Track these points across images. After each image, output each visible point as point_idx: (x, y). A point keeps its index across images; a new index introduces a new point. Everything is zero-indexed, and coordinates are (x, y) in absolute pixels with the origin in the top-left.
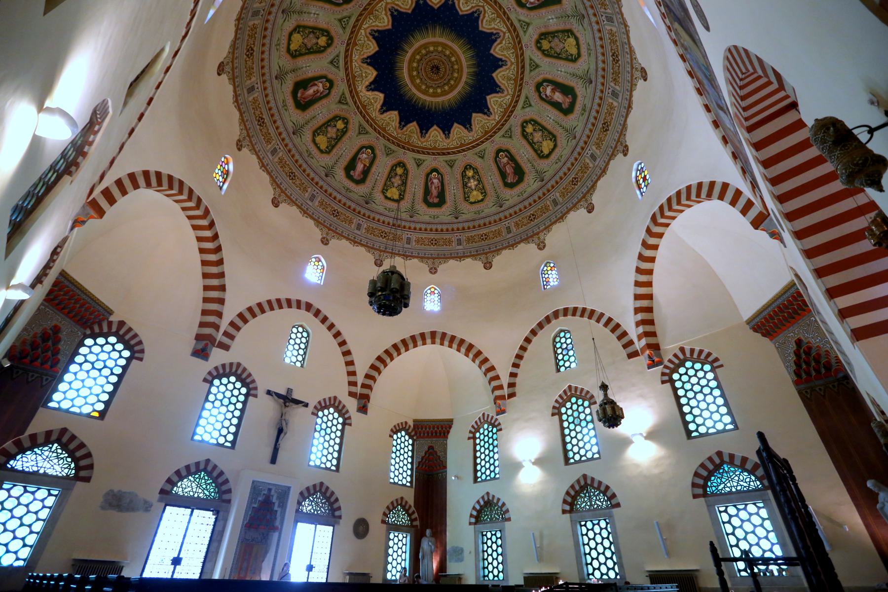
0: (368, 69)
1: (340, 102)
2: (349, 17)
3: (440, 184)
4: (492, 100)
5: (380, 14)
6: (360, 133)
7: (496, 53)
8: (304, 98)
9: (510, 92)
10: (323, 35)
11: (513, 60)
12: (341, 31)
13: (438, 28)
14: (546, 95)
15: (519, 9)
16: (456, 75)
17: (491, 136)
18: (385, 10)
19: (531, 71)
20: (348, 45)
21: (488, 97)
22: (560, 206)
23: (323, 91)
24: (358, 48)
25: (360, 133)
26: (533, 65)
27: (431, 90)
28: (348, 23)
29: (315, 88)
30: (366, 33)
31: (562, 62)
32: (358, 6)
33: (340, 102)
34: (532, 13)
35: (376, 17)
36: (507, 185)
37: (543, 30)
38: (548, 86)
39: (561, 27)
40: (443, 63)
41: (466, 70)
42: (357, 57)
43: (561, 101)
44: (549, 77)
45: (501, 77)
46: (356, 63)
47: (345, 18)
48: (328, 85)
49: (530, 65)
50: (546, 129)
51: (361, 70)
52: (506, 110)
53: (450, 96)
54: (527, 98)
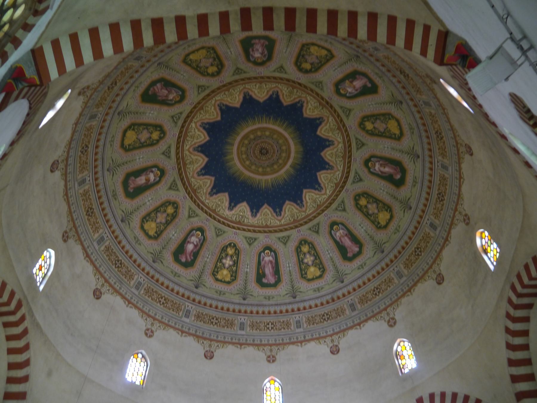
0: (329, 160)
1: (363, 144)
2: (337, 209)
3: (251, 53)
4: (203, 137)
6: (350, 110)
7: (208, 179)
8: (395, 170)
9: (187, 153)
10: (361, 206)
11: (193, 180)
12: (346, 201)
14: (152, 172)
15: (200, 224)
16: (243, 149)
17: (195, 107)
18: (307, 206)
19: (174, 181)
20: (343, 187)
21: (208, 138)
22: (86, 122)
23: (377, 162)
25: (350, 110)
27: (267, 133)
29: (382, 169)
30: (326, 190)
31: (152, 208)
33: (363, 144)
34: (189, 228)
35: (315, 201)
36: (162, 80)
37: (177, 220)
38: (155, 180)
39: (164, 235)
40: (257, 157)
41: (235, 155)
42: (337, 173)
43: (138, 179)
44: (158, 187)
48: (370, 164)
49: (177, 185)
50: (140, 148)
51: (336, 161)
52: (186, 135)
53: (246, 130)
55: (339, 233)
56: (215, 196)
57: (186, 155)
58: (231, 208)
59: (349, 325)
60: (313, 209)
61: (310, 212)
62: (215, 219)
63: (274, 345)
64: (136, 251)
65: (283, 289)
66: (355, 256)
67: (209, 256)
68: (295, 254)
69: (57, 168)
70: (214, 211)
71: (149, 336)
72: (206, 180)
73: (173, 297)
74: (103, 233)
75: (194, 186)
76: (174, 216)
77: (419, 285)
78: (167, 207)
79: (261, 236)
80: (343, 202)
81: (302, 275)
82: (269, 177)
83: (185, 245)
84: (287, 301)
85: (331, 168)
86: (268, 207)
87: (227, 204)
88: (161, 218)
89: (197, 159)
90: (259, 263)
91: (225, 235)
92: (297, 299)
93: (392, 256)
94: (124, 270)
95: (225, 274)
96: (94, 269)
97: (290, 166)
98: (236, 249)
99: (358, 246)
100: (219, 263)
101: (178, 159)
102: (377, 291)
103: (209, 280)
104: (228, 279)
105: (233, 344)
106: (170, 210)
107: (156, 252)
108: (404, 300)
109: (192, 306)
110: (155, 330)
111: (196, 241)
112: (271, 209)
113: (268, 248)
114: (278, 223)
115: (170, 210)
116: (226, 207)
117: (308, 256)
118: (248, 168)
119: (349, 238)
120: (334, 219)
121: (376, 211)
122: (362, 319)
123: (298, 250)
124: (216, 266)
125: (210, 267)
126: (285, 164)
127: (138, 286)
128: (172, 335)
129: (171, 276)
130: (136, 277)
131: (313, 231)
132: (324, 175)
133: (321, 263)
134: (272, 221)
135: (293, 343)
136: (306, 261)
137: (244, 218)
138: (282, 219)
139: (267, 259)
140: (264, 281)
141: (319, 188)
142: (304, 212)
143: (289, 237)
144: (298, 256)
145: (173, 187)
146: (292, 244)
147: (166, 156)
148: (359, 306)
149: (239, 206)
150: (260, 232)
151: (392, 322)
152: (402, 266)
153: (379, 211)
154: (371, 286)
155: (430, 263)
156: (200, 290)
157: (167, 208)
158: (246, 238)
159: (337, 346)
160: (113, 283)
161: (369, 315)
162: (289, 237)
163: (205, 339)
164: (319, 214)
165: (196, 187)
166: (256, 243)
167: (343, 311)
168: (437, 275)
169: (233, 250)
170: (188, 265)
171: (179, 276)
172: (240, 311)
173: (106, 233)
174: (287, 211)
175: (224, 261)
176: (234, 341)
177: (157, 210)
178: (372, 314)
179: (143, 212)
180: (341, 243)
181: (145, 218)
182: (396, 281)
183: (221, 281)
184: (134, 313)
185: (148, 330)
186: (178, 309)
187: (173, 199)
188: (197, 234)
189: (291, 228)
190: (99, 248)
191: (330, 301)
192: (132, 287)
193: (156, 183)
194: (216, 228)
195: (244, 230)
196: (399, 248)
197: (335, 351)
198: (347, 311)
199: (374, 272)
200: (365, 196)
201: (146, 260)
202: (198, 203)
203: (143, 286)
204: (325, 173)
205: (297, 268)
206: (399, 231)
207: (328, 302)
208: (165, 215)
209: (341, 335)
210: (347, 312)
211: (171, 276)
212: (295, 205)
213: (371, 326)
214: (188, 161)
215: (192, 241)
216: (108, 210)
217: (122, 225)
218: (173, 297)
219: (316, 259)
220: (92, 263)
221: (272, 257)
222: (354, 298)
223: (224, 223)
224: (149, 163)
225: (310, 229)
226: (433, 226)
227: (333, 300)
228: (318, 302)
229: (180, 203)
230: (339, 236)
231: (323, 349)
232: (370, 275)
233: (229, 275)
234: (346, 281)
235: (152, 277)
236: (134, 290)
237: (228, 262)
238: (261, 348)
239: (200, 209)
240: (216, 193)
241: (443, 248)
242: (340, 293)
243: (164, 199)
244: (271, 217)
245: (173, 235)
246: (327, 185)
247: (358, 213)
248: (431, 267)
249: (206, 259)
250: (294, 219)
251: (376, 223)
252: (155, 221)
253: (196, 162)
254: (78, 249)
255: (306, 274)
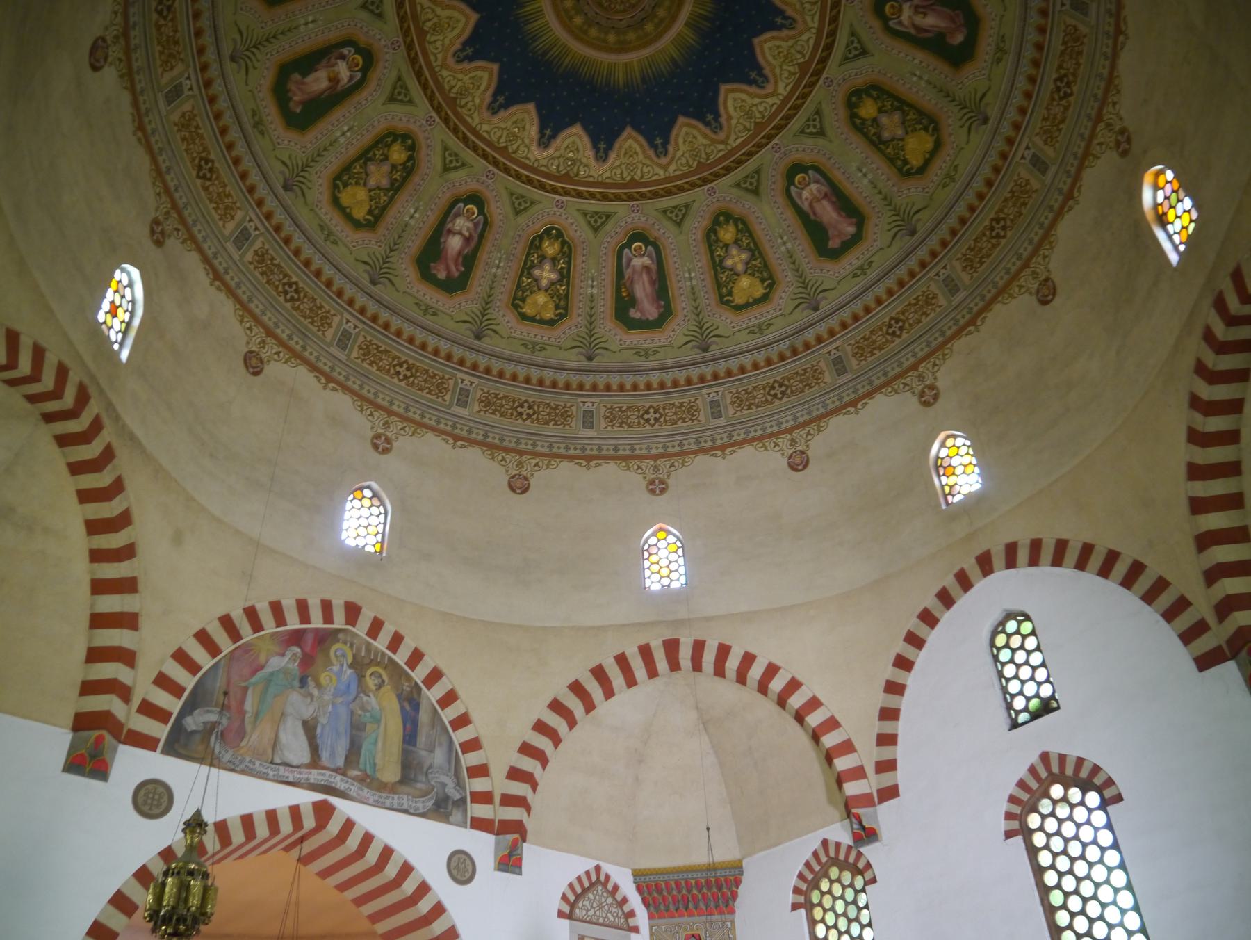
2: (802, 132)
5: (741, 121)
7: (483, 69)
11: (445, 73)
12: (826, 109)
13: (621, 83)
14: (343, 57)
15: (473, 186)
18: (729, 126)
19: (399, 79)
20: (818, 73)
24: (799, 56)
26: (399, 93)
28: (808, 120)
29: (919, 20)
30: (776, 83)
31: (353, 152)
32: (783, 150)
34: (445, 198)
35: (748, 114)
37: (416, 179)
38: (351, 78)
39: (390, 217)
42: (805, 37)
43: (309, 79)
44: (362, 96)
45: (458, 21)
46: (811, 25)
47: (811, 133)
49: (407, 89)
54: (380, 16)
55: (809, 192)
56: (502, 113)
57: (422, 7)
58: (544, 142)
59: (831, 406)
60: (745, 135)
61: (739, 141)
62: (507, 170)
63: (662, 456)
64: (328, 260)
65: (678, 331)
66: (849, 244)
67: (500, 262)
68: (703, 248)
69: (106, 58)
70: (503, 151)
71: (383, 450)
72: (479, 73)
73: (425, 362)
74: (243, 219)
75: (450, 90)
76: (409, 169)
77: (997, 307)
78: (389, 146)
79: (620, 208)
80: (818, 112)
81: (721, 296)
82: (632, 57)
83: (442, 240)
84: (689, 358)
85: (790, 23)
86: (634, 134)
87: (533, 131)
88: (378, 175)
89: (450, 18)
90: (620, 274)
91: (536, 208)
92: (711, 353)
93: (933, 242)
94: (306, 306)
95: (540, 302)
96: (238, 306)
97: (686, 24)
98: (564, 243)
99: (854, 220)
100: (524, 279)
101: (402, 19)
102: (896, 326)
103: (505, 320)
104: (549, 315)
105: (572, 458)
106: (398, 154)
107: (375, 259)
108: (959, 344)
109: (473, 379)
110: (393, 437)
111: (468, 229)
112: (641, 138)
113: (638, 236)
114: (661, 172)
115: (398, 154)
116: (532, 140)
117: (734, 251)
118: (580, 35)
119: (833, 203)
120: (798, 156)
121: (900, 132)
122: (861, 391)
123: (711, 235)
124: (519, 286)
125: (505, 288)
126: (674, 19)
127: (344, 340)
128: (433, 445)
129: (416, 314)
130: (336, 320)
131: (746, 189)
132: (770, 44)
133: (766, 266)
134: (645, 170)
135: (705, 451)
136: (729, 262)
137: (576, 167)
138: (669, 164)
139: (637, 262)
140: (634, 314)
141: (760, 80)
142: (722, 142)
143: (687, 206)
144: (712, 252)
145: (398, 95)
146: (697, 224)
147: (372, 12)
148: (854, 362)
149: (563, 135)
150: (617, 198)
151: (929, 394)
152: (958, 265)
153: (907, 133)
154: (882, 315)
155: (1025, 255)
156: (486, 343)
157: (388, 150)
158: (585, 214)
159: (803, 452)
160: (284, 336)
161: (877, 383)
162: (687, 206)
163: (507, 450)
164: (760, 146)
165: (454, 90)
166: (608, 227)
167: (817, 374)
168: (1040, 284)
169: (557, 246)
170: (453, 286)
171: (434, 314)
172: (581, 387)
173: (251, 220)
174: (681, 141)
175: (537, 272)
176: (572, 452)
177: (365, 156)
178: (883, 379)
179: (333, 162)
180: (812, 217)
181: (338, 177)
182: (942, 301)
183: (533, 319)
184: (343, 402)
185: (378, 437)
186: (441, 388)
187: (401, 126)
188: (468, 210)
189: (693, 185)
190: (242, 256)
191: (788, 354)
192: (330, 345)
193: (356, 87)
194: (512, 194)
195: (579, 195)
196: (952, 221)
197: (799, 463)
198: (827, 374)
199: (891, 282)
200: (874, 93)
201: (354, 281)
202: (463, 133)
203: (355, 340)
204: (773, 38)
205: (709, 283)
206: (954, 181)
207: (782, 357)
208: (386, 168)
209: (812, 428)
210: (827, 377)
211: (416, 314)
212: (701, 126)
213: (881, 404)
214: (429, 24)
215: (457, 228)
216: (247, 163)
217: (287, 197)
218: (425, 362)
219: (753, 257)
220: (231, 293)
221: (650, 256)
222: (844, 344)
223: (529, 181)
224: (333, 36)
225: (738, 185)
226: (1039, 164)
227: (795, 352)
228: (760, 357)
229: (421, 137)
230: (810, 198)
231: (773, 460)
232: (880, 290)
233: (552, 306)
234: (825, 307)
235: (374, 319)
236: (334, 350)
237: (546, 274)
238: (634, 465)
239: (468, 147)
240: (506, 106)
241: (1059, 214)
242: (810, 335)
243: (380, 127)
244: (644, 162)
245: (412, 217)
246: (778, 71)
247: (856, 139)
248: (1026, 265)
249: (494, 270)
250: (699, 162)
251: (899, 163)
252: (365, 185)
253: (449, 26)
254: (191, 260)
255: (730, 293)
